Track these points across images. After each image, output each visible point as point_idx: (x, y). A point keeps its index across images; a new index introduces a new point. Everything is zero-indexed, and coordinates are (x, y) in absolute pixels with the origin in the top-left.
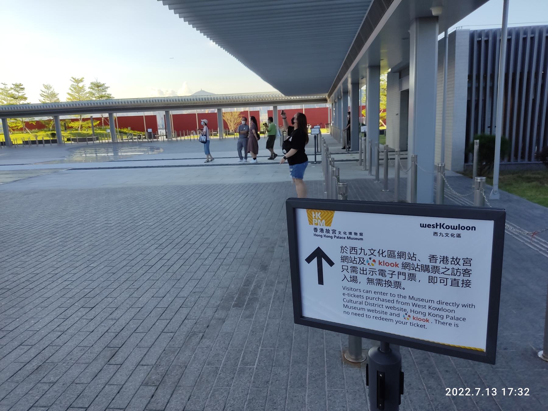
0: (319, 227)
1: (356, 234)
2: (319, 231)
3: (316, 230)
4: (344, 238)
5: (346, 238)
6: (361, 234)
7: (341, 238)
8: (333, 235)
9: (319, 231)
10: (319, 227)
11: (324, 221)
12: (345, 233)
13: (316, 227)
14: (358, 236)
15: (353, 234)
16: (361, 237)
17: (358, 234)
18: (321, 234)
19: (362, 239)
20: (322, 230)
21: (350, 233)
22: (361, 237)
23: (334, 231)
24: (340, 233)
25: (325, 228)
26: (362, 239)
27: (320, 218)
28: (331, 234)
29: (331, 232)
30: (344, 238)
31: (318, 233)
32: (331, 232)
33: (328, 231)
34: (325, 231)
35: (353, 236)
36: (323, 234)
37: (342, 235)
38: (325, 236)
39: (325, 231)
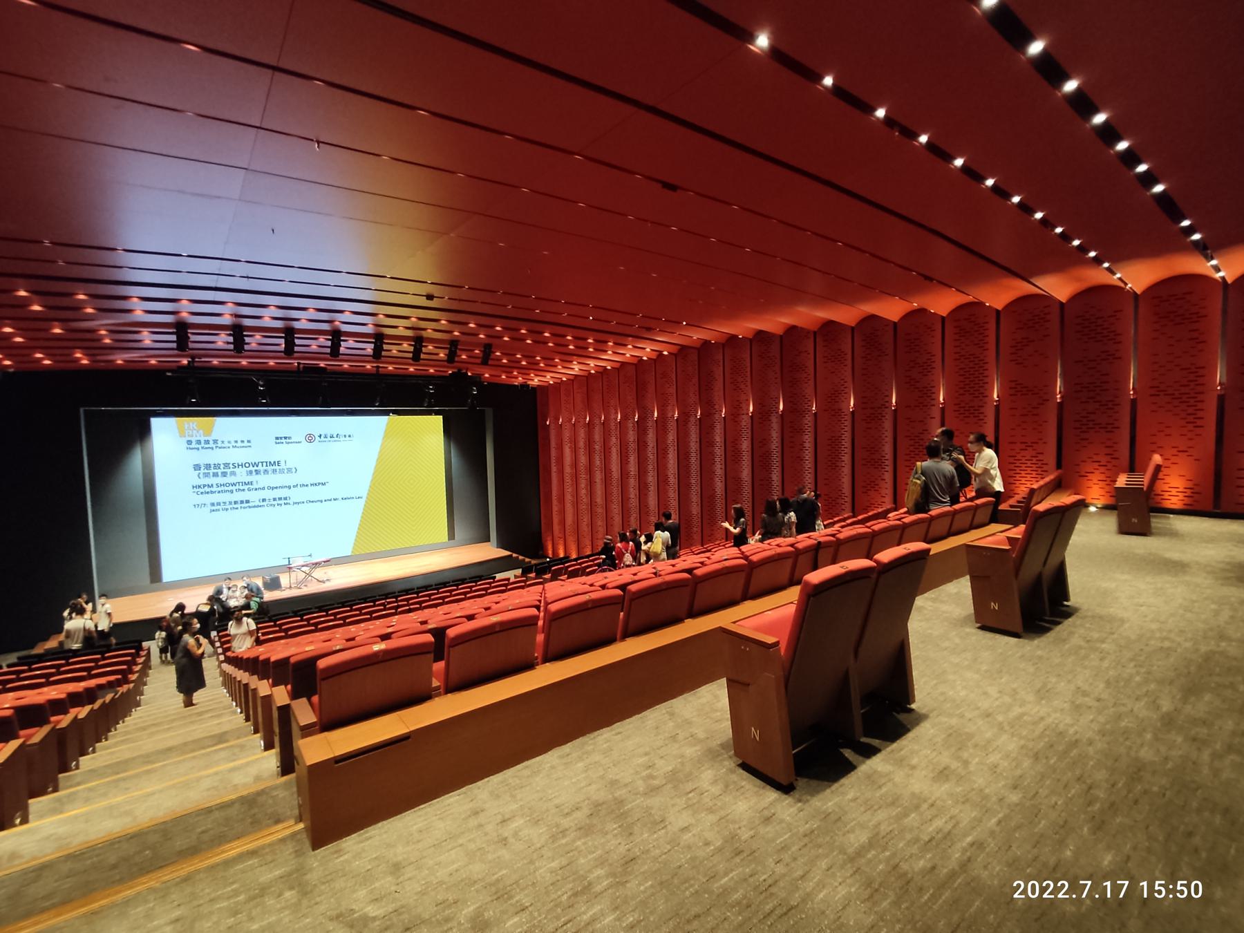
0: (194, 439)
1: (242, 441)
2: (194, 443)
3: (189, 442)
4: (229, 447)
5: (231, 447)
6: (249, 441)
7: (224, 448)
8: (214, 446)
9: (194, 443)
10: (194, 439)
11: (201, 432)
12: (229, 442)
13: (189, 439)
14: (246, 444)
15: (239, 442)
16: (249, 444)
17: (246, 442)
18: (197, 446)
19: (250, 446)
20: (199, 442)
21: (236, 442)
22: (249, 444)
23: (215, 441)
24: (223, 442)
25: (202, 439)
26: (250, 446)
27: (195, 428)
28: (211, 444)
29: (211, 442)
30: (229, 447)
31: (193, 445)
32: (211, 442)
33: (207, 442)
34: (203, 442)
35: (239, 444)
36: (200, 446)
37: (226, 444)
38: (202, 448)
39: (203, 442)
